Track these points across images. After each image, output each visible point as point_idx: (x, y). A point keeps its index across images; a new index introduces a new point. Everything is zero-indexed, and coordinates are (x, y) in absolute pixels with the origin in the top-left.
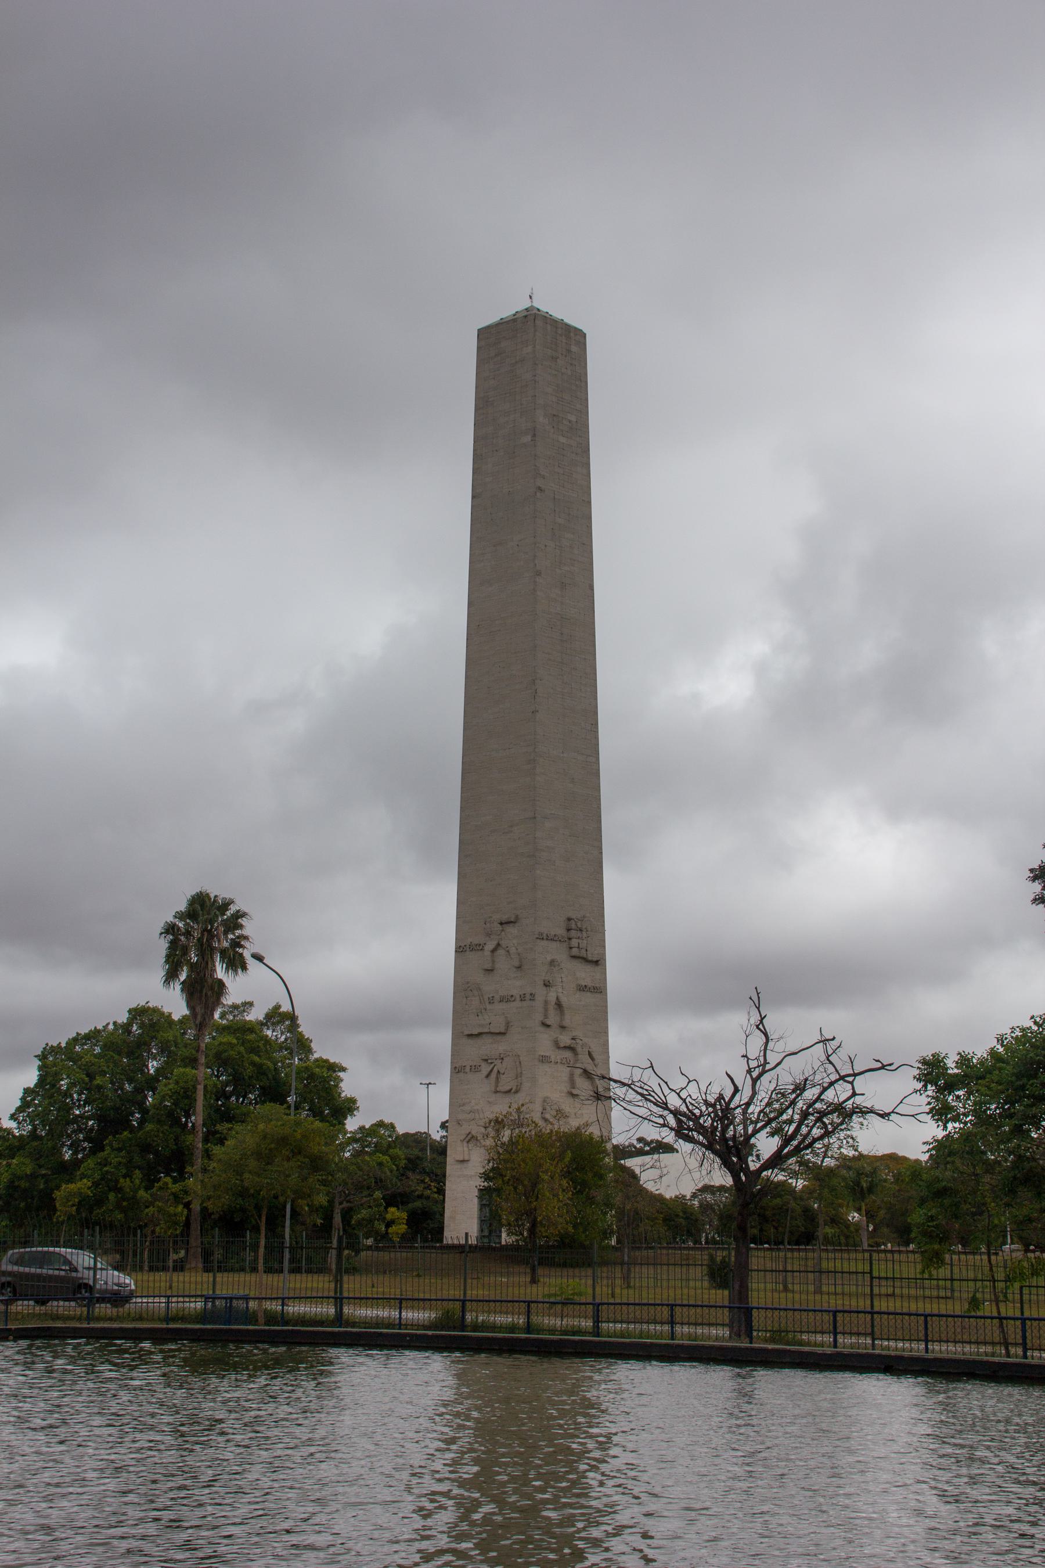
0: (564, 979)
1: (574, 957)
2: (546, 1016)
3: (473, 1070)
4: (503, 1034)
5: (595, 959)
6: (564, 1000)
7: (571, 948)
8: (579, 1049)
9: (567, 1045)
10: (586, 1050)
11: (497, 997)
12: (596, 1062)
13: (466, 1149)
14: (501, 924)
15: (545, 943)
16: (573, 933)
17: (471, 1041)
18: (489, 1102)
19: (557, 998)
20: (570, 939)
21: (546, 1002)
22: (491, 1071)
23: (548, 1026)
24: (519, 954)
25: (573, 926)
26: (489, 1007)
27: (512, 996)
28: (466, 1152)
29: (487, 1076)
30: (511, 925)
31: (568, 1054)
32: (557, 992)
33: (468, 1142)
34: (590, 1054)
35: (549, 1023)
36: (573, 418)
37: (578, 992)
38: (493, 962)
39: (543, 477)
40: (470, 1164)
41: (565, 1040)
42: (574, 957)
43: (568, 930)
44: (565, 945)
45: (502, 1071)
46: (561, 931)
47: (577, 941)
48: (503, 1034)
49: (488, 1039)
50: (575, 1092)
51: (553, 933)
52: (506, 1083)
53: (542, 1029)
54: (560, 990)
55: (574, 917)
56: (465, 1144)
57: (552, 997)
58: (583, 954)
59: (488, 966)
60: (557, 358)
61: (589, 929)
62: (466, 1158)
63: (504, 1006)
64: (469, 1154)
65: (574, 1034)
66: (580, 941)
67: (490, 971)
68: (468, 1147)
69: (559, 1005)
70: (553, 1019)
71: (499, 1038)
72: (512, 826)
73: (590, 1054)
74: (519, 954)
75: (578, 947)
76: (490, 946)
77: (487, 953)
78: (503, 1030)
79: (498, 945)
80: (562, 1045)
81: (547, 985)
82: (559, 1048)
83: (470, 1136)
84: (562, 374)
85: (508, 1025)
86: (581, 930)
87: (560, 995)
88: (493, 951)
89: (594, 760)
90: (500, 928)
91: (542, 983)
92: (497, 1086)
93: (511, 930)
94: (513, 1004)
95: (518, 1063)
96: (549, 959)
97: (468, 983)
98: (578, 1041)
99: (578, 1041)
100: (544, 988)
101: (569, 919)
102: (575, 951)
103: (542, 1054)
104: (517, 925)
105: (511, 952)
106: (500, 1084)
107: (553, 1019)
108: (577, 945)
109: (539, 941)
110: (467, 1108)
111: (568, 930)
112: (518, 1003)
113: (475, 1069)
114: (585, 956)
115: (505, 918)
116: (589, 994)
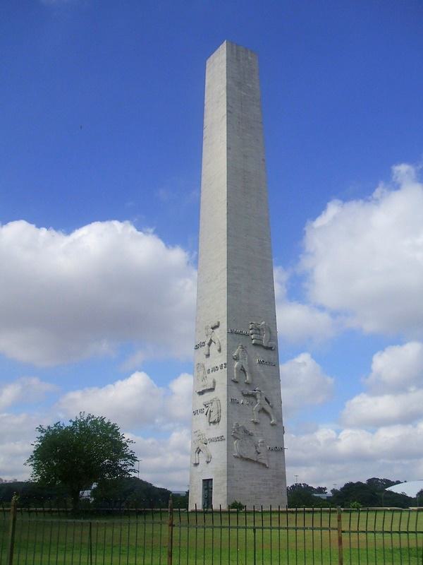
4: (212, 390)
8: (258, 396)
10: (263, 397)
14: (213, 328)
26: (208, 375)
31: (252, 399)
34: (266, 399)
38: (209, 350)
52: (214, 418)
59: (207, 353)
73: (266, 399)
77: (206, 346)
78: (212, 387)
79: (211, 341)
82: (244, 395)
85: (214, 382)
92: (209, 419)
93: (217, 330)
113: (202, 411)
115: (213, 325)
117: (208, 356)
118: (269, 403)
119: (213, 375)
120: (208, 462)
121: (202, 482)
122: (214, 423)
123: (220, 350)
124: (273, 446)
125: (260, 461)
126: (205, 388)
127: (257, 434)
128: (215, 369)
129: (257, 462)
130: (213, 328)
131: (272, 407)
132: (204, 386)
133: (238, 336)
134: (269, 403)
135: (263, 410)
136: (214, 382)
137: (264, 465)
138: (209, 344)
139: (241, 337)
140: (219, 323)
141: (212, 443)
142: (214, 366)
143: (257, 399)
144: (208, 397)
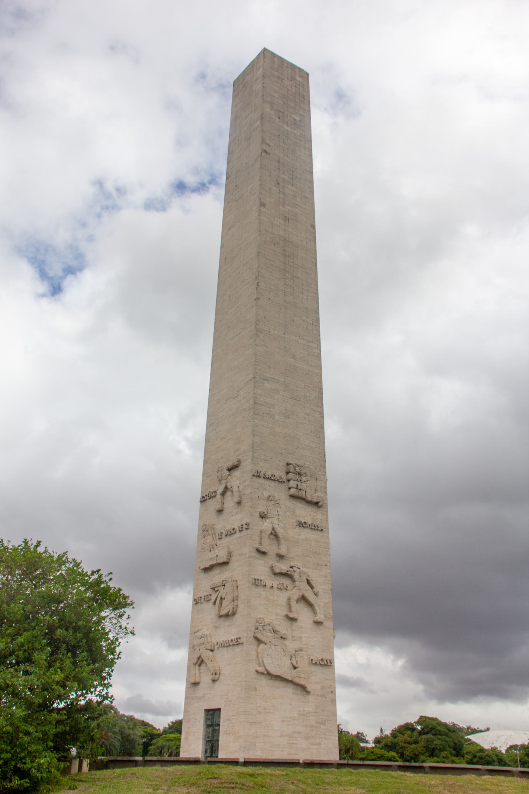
0: (280, 513)
1: (292, 496)
2: (261, 543)
3: (206, 599)
4: (225, 564)
5: (315, 500)
6: (280, 532)
7: (290, 488)
8: (296, 576)
9: (284, 572)
10: (304, 578)
11: (224, 533)
12: (315, 590)
13: (197, 672)
15: (262, 481)
16: (291, 476)
17: (206, 575)
18: (215, 627)
19: (273, 529)
20: (289, 481)
21: (261, 532)
22: (218, 596)
23: (264, 553)
24: (240, 492)
25: (292, 470)
26: (219, 542)
27: (234, 529)
28: (198, 675)
29: (214, 603)
30: (236, 470)
31: (286, 581)
32: (273, 523)
33: (200, 665)
34: (308, 582)
35: (263, 550)
36: (298, 119)
37: (297, 528)
38: (223, 503)
39: (269, 145)
40: (201, 686)
41: (283, 567)
42: (292, 496)
43: (288, 473)
44: (284, 486)
45: (223, 597)
46: (283, 475)
47: (296, 482)
48: (225, 564)
49: (216, 571)
50: (291, 615)
51: (270, 474)
53: (256, 554)
54: (276, 522)
55: (293, 463)
56: (197, 667)
57: (267, 525)
58: (302, 494)
59: (218, 507)
60: (283, 79)
61: (308, 474)
62: (197, 681)
63: (228, 539)
64: (200, 677)
65: (292, 564)
66: (299, 483)
67: (220, 511)
68: (199, 670)
69: (274, 535)
70: (267, 545)
71: (224, 568)
72: (239, 391)
73: (308, 582)
74: (240, 492)
75: (297, 488)
76: (221, 490)
77: (219, 496)
78: (225, 559)
79: (226, 488)
80: (277, 571)
81: (263, 516)
82: (275, 574)
83: (200, 660)
84: (288, 90)
85: (230, 554)
86: (299, 474)
87: (276, 526)
88: (223, 494)
89: (316, 346)
90: (228, 473)
91: (258, 514)
92: (219, 611)
93: (236, 473)
94: (234, 537)
95: (235, 587)
96: (266, 494)
97: (206, 525)
98: (295, 569)
99: (295, 569)
100: (260, 519)
101: (288, 464)
102: (293, 491)
103: (257, 577)
104: (239, 468)
105: (234, 491)
106: (222, 608)
107: (267, 545)
108: (295, 486)
109: (255, 478)
110: (199, 634)
111: (288, 473)
112: (238, 534)
114: (304, 496)
115: (230, 464)
116: (309, 530)
117: (220, 511)
118: (312, 587)
119: (226, 541)
120: (214, 681)
121: (203, 711)
122: (227, 616)
123: (239, 503)
124: (317, 656)
125: (297, 680)
126: (214, 562)
127: (293, 637)
128: (231, 533)
129: (291, 682)
130: (229, 470)
131: (316, 594)
132: (212, 559)
133: (267, 482)
134: (312, 587)
135: (303, 599)
136: (230, 554)
137: (303, 688)
138: (223, 494)
139: (272, 484)
140: (239, 462)
141: (224, 651)
142: (229, 527)
143: (294, 581)
144: (217, 577)
